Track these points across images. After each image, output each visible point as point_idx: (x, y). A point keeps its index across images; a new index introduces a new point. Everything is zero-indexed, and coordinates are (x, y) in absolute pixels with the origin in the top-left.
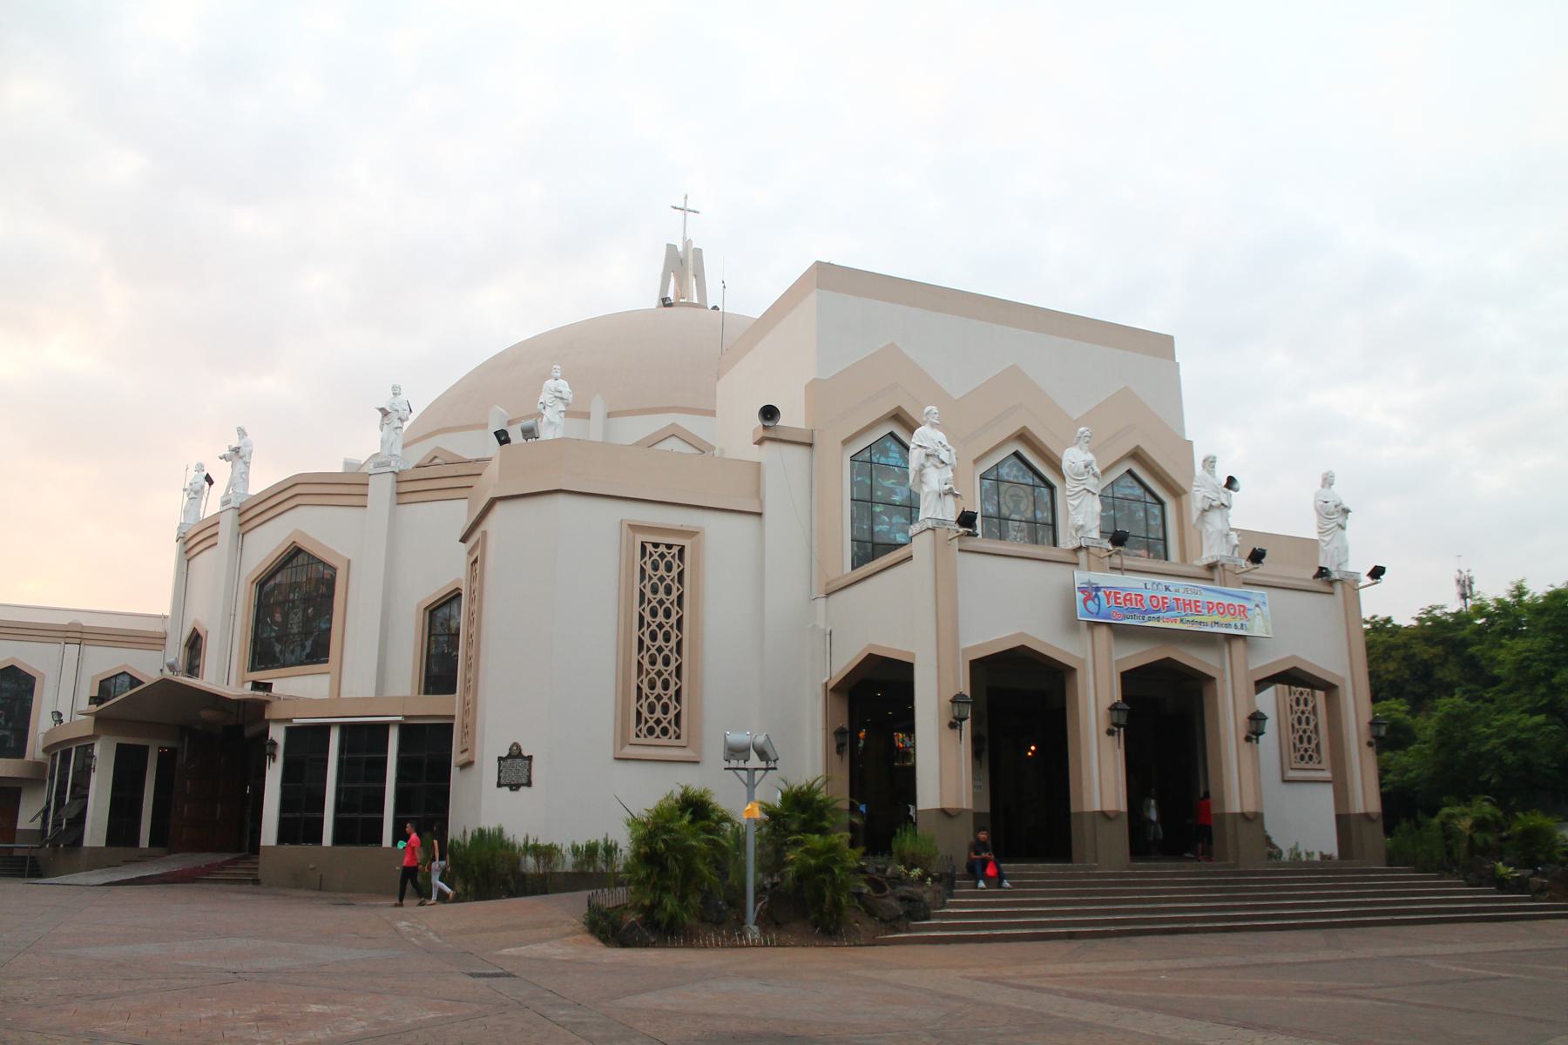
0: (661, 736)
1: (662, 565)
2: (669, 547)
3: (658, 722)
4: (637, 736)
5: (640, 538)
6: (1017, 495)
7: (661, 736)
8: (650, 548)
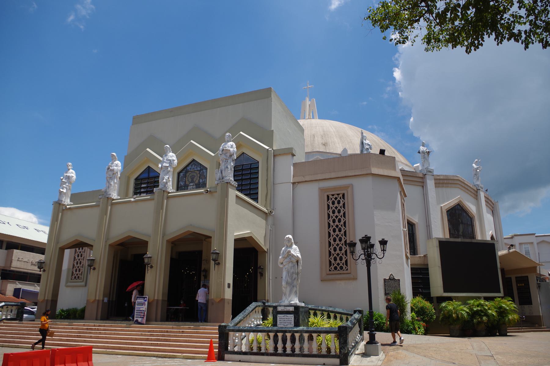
6: (194, 176)
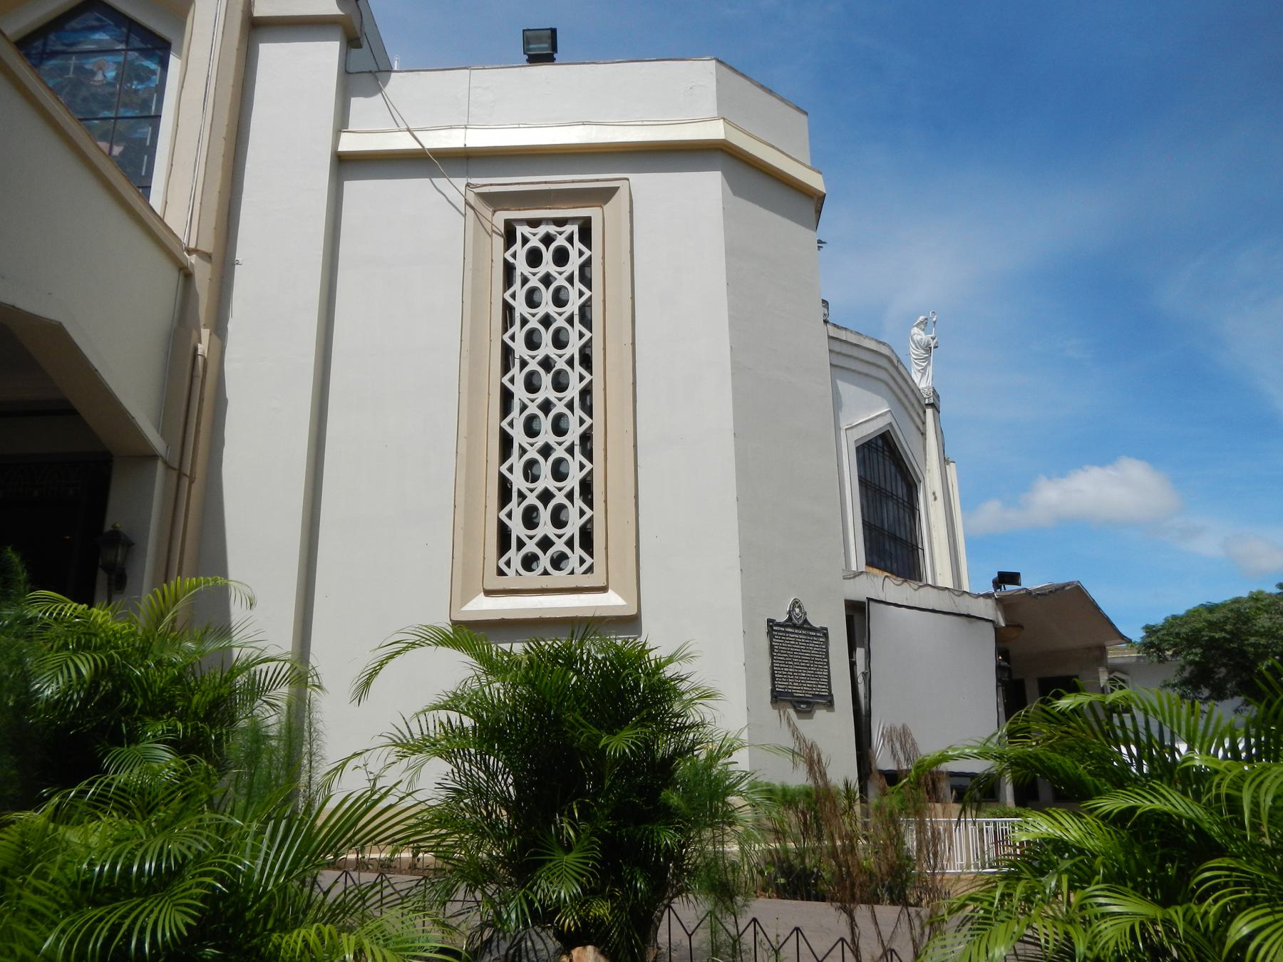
0: (550, 569)
1: (548, 256)
2: (560, 222)
3: (545, 543)
4: (501, 573)
5: (501, 217)
7: (550, 569)
8: (521, 230)
